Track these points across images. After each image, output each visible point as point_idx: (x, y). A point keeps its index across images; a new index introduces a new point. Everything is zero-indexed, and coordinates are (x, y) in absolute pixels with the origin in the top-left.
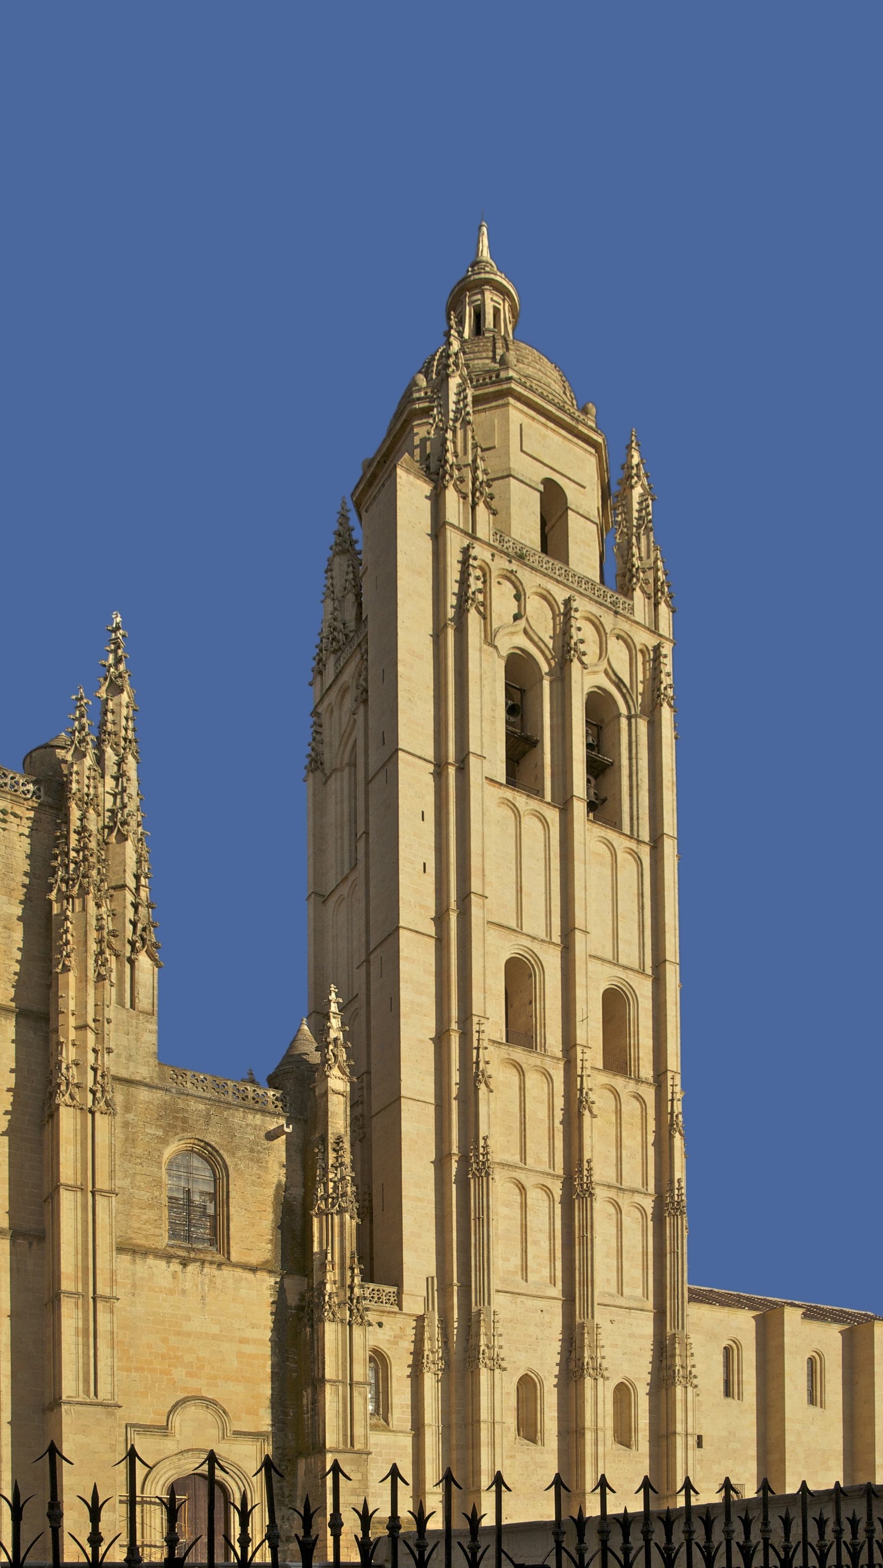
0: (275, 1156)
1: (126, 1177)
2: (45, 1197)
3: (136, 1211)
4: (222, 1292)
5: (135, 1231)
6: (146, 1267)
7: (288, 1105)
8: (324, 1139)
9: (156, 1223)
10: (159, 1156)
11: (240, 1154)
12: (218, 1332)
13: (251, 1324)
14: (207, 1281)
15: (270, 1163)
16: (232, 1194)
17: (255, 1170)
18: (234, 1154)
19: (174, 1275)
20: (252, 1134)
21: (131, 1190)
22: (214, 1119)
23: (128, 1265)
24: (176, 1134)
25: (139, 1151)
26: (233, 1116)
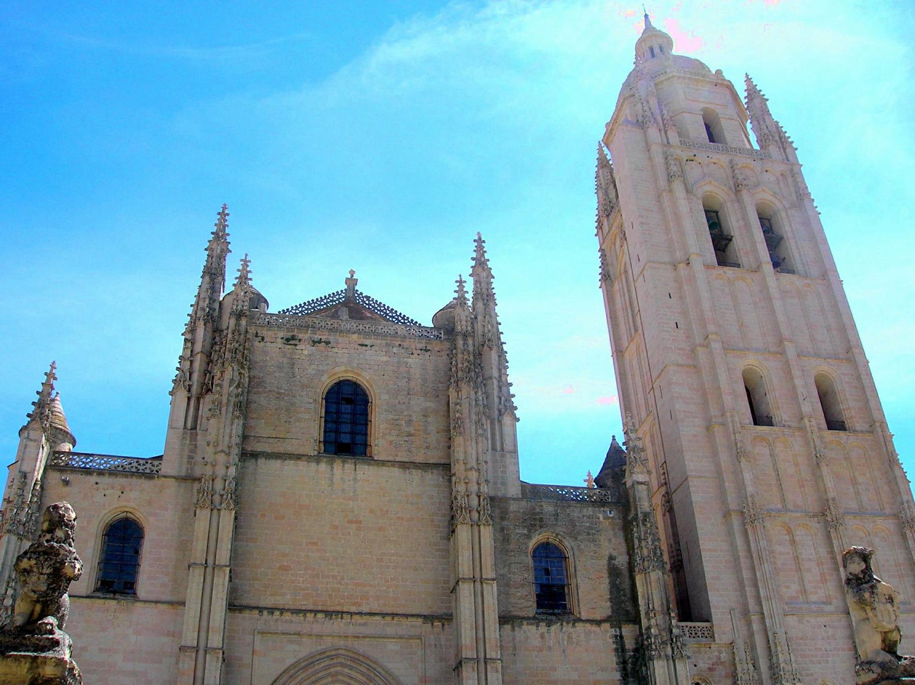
0: (605, 536)
1: (505, 566)
2: (452, 589)
3: (513, 590)
4: (577, 645)
5: (513, 605)
6: (522, 632)
7: (610, 497)
8: (636, 518)
9: (527, 597)
10: (526, 548)
11: (580, 538)
12: (577, 678)
13: (601, 668)
14: (566, 638)
15: (602, 541)
16: (578, 568)
17: (593, 548)
18: (576, 538)
19: (542, 636)
20: (587, 522)
21: (509, 576)
22: (561, 516)
23: (510, 632)
24: (536, 530)
25: (512, 547)
26: (573, 511)
